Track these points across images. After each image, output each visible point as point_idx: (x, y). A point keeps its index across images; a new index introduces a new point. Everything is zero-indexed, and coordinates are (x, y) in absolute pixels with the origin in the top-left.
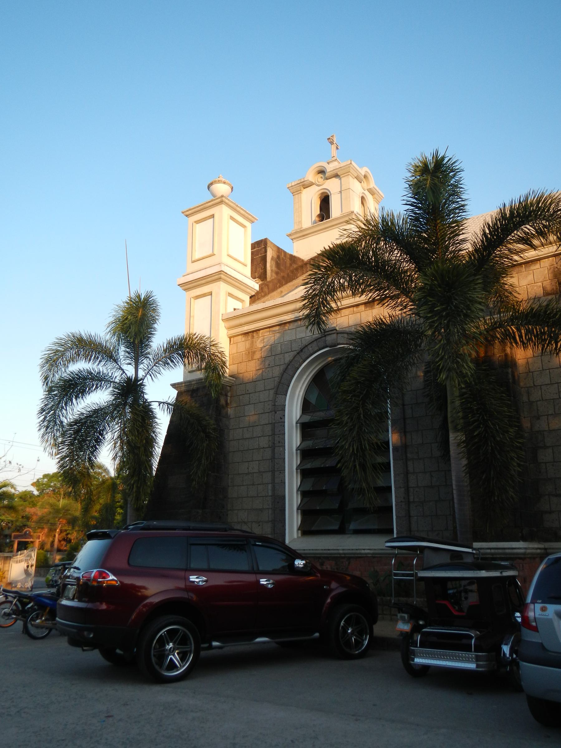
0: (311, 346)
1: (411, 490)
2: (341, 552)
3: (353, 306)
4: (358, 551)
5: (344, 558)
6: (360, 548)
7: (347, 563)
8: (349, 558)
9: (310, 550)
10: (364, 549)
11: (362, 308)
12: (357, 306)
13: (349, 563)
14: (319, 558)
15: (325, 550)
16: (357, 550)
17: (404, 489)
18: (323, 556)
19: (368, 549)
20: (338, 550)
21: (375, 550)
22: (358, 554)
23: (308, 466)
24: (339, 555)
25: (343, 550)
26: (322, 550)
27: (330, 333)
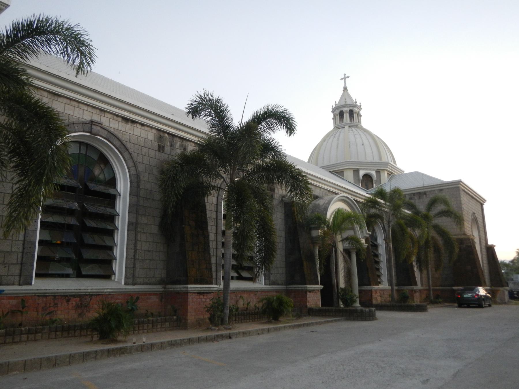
0: (77, 125)
1: (138, 251)
2: (89, 291)
3: (114, 115)
4: (102, 290)
5: (87, 295)
6: (105, 288)
7: (89, 299)
8: (92, 295)
9: (63, 289)
10: (107, 289)
11: (120, 119)
12: (117, 116)
13: (91, 299)
14: (67, 296)
15: (77, 289)
16: (102, 289)
17: (134, 250)
18: (70, 294)
19: (111, 289)
20: (88, 289)
21: (115, 289)
22: (101, 292)
23: (50, 219)
24: (84, 294)
25: (92, 289)
26: (74, 289)
27: (97, 124)
